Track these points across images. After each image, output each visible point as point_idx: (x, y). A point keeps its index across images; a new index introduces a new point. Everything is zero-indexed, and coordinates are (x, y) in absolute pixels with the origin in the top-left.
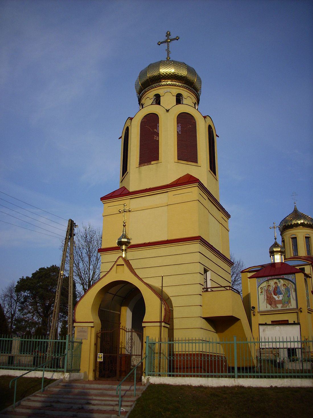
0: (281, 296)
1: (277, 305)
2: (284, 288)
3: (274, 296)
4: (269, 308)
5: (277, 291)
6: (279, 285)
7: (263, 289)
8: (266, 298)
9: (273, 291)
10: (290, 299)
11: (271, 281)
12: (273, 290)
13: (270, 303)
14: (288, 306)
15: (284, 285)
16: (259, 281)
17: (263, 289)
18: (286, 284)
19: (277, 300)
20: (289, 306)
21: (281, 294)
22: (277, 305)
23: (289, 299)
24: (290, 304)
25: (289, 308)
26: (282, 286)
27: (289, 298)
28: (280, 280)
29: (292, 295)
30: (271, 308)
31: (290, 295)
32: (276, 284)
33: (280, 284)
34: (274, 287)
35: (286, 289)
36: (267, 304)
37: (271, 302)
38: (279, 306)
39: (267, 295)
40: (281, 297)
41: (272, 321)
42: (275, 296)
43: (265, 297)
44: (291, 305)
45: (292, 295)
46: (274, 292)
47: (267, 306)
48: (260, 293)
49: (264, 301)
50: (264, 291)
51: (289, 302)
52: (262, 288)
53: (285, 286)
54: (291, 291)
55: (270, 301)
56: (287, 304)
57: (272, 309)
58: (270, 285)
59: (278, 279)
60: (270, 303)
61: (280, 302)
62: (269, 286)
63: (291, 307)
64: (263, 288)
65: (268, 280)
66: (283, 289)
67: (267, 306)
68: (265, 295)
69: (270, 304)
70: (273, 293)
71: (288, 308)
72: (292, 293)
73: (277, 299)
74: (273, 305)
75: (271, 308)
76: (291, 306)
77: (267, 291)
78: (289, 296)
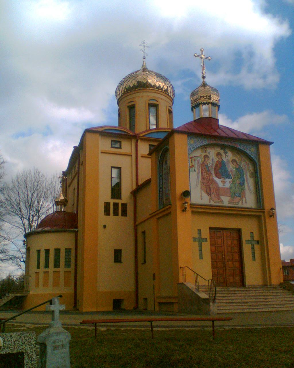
0: (228, 180)
1: (222, 198)
2: (233, 167)
3: (216, 179)
4: (206, 200)
5: (221, 170)
6: (225, 159)
7: (194, 160)
8: (200, 179)
10: (243, 189)
12: (214, 166)
14: (240, 203)
15: (234, 161)
16: (192, 141)
17: (194, 160)
18: (238, 161)
21: (228, 176)
22: (221, 197)
23: (242, 189)
24: (244, 199)
26: (231, 162)
27: (243, 186)
28: (227, 150)
29: (248, 183)
32: (219, 157)
33: (227, 158)
34: (216, 160)
35: (237, 169)
37: (210, 190)
38: (226, 201)
40: (228, 183)
41: (211, 228)
43: (198, 177)
44: (246, 201)
45: (248, 183)
47: (201, 196)
49: (197, 185)
50: (196, 166)
52: (192, 157)
54: (246, 176)
55: (209, 188)
56: (239, 198)
57: (212, 203)
58: (208, 155)
59: (223, 147)
62: (206, 157)
63: (245, 205)
64: (195, 158)
65: (204, 147)
66: (231, 167)
67: (201, 196)
68: (198, 173)
69: (209, 194)
70: (213, 172)
71: (240, 205)
72: (247, 179)
73: (221, 185)
74: (212, 196)
76: (246, 202)
77: (204, 167)
78: (242, 184)
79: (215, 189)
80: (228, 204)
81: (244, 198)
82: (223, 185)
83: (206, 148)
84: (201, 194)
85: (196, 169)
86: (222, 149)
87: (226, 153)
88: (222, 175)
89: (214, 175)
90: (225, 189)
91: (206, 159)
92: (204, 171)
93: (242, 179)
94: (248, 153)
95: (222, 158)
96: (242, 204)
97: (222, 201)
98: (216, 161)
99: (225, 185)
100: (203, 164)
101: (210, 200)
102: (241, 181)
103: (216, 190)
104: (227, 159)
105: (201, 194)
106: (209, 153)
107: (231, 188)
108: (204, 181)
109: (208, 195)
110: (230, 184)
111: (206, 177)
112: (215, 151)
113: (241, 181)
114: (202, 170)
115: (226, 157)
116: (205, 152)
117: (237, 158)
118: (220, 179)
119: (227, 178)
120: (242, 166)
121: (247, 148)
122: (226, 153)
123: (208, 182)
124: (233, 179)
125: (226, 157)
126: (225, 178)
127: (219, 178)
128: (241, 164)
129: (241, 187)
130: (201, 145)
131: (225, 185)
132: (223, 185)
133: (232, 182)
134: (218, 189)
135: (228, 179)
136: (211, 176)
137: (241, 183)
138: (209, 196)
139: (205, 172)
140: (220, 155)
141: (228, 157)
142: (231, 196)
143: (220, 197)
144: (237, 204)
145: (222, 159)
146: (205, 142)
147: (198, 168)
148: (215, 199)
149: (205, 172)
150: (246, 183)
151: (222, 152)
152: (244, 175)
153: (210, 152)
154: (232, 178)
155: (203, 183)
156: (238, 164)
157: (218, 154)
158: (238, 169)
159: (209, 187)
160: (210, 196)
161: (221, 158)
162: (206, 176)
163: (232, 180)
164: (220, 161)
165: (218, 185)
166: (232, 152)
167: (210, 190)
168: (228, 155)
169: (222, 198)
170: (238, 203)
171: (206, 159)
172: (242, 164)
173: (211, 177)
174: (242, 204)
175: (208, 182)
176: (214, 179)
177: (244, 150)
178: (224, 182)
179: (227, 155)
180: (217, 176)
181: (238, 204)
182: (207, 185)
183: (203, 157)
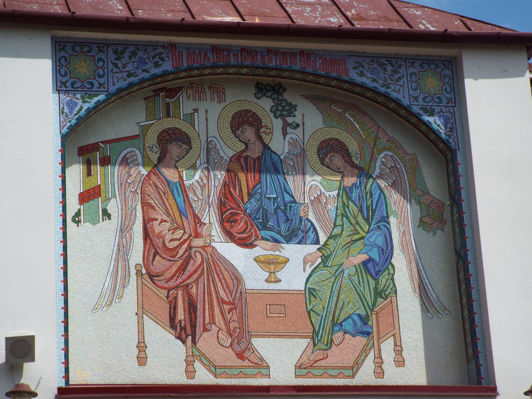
0: (295, 253)
6: (279, 145)
8: (137, 255)
9: (214, 199)
11: (200, 96)
13: (181, 315)
18: (353, 146)
19: (260, 294)
20: (379, 363)
21: (297, 231)
22: (256, 342)
23: (379, 293)
24: (387, 347)
25: (380, 382)
27: (383, 280)
30: (190, 373)
31: (387, 252)
32: (249, 133)
33: (292, 134)
36: (147, 320)
37: (192, 308)
39: (157, 228)
42: (232, 246)
43: (122, 251)
44: (398, 349)
46: (222, 207)
47: (142, 346)
48: (73, 205)
49: (115, 294)
51: (369, 324)
52: (95, 147)
53: (338, 161)
57: (204, 377)
58: (185, 127)
60: (181, 315)
61: (280, 313)
64: (108, 151)
67: (142, 346)
68: (124, 229)
69: (186, 330)
70: (211, 218)
71: (365, 376)
73: (254, 278)
74: (206, 342)
75: (190, 373)
76: (400, 362)
78: (377, 267)
79: (221, 302)
80: (297, 376)
81: (391, 341)
82: (267, 281)
83: (172, 92)
84: (141, 332)
85: (113, 207)
86: (261, 89)
87: (284, 110)
88: (264, 227)
89: (216, 231)
90: (277, 302)
91: (174, 150)
92: (159, 214)
93: (380, 241)
94: (405, 102)
95: (264, 136)
96: (380, 372)
97: (261, 366)
98: (231, 153)
99: (278, 281)
100: (154, 178)
101: (189, 363)
102: (375, 255)
103: (227, 307)
104: (293, 143)
105: (141, 332)
106: (190, 119)
107: (311, 292)
108: (159, 264)
109: (179, 338)
110: (309, 270)
111: (171, 245)
112: (223, 105)
113: (375, 255)
114: (145, 205)
115: (285, 134)
116: (168, 115)
117: (352, 130)
118: (251, 246)
119: (288, 239)
120: (377, 171)
121: (398, 80)
122: (284, 110)
123: (183, 268)
124: (325, 244)
125: (285, 134)
126: (276, 241)
127: (245, 243)
128: (373, 159)
129: (372, 282)
130: (132, 79)
131: (278, 281)
132: (267, 281)
133: (319, 260)
134: (237, 299)
135: (299, 243)
136: (198, 235)
137: (370, 260)
138: (184, 342)
139: (165, 218)
140: (251, 125)
141: (300, 130)
142: (314, 336)
143: (250, 342)
144: (349, 373)
145: (266, 147)
146: (157, 65)
147: (125, 202)
148: (228, 357)
149: (165, 218)
150: (400, 261)
151: (264, 106)
152: (393, 220)
153: (196, 110)
154: (323, 239)
155: (151, 276)
156: (357, 162)
157: (243, 120)
158: (355, 195)
159: (190, 295)
160: (194, 342)
161: (260, 138)
162: (168, 237)
163: (319, 249)
164: (255, 151)
165: (238, 278)
166: (315, 99)
167: (192, 308)
168: (298, 120)
169: (263, 346)
170: (355, 368)
171: (174, 150)
172: (378, 164)
173: (198, 242)
174: (380, 372)
175: (183, 268)
176: (214, 248)
177: (383, 90)
178: (272, 265)
179: (290, 120)
180: (230, 236)
181: (353, 377)
182: (172, 284)
183: (152, 139)
